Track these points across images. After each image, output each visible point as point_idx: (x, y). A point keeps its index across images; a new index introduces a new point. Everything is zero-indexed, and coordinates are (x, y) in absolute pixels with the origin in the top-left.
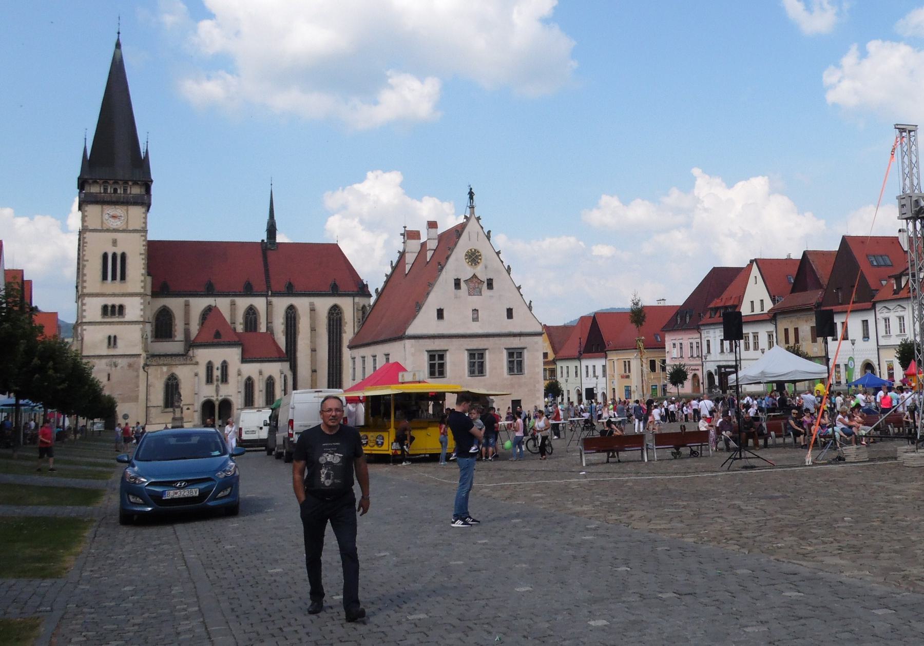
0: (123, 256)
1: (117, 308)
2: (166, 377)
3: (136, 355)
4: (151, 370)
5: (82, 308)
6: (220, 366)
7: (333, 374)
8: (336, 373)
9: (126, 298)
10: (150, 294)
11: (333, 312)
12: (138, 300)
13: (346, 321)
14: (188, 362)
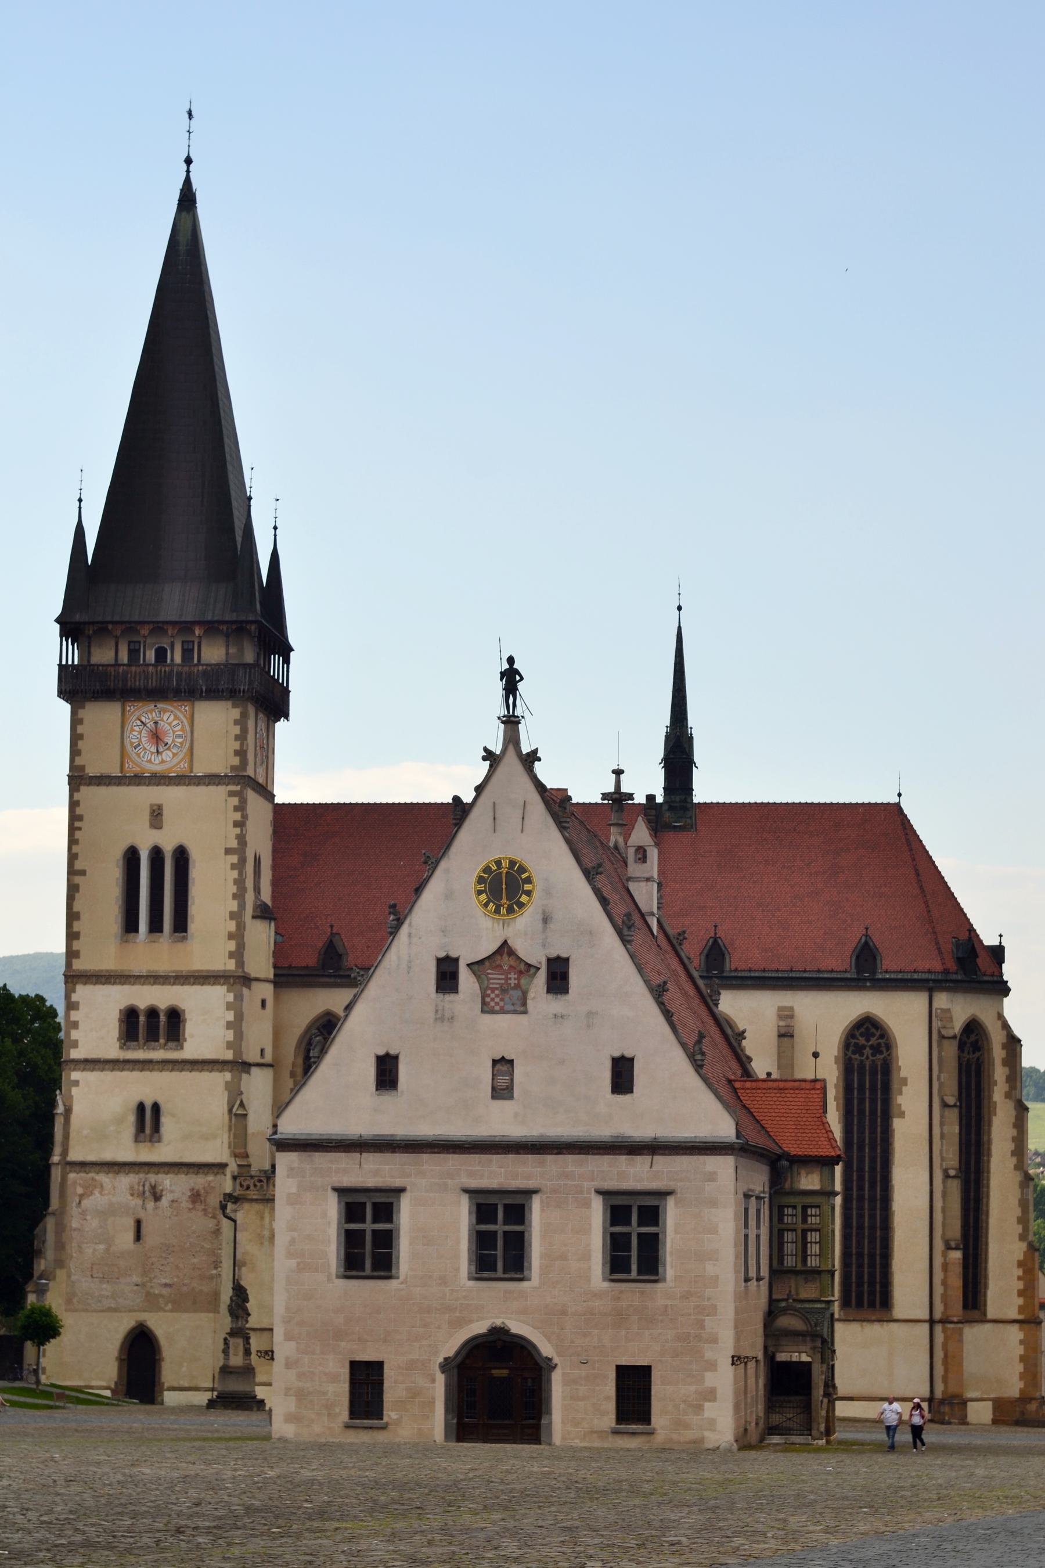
1: (163, 1018)
7: (860, 1255)
8: (872, 1256)
10: (271, 976)
11: (862, 1041)
12: (218, 995)
13: (903, 1074)
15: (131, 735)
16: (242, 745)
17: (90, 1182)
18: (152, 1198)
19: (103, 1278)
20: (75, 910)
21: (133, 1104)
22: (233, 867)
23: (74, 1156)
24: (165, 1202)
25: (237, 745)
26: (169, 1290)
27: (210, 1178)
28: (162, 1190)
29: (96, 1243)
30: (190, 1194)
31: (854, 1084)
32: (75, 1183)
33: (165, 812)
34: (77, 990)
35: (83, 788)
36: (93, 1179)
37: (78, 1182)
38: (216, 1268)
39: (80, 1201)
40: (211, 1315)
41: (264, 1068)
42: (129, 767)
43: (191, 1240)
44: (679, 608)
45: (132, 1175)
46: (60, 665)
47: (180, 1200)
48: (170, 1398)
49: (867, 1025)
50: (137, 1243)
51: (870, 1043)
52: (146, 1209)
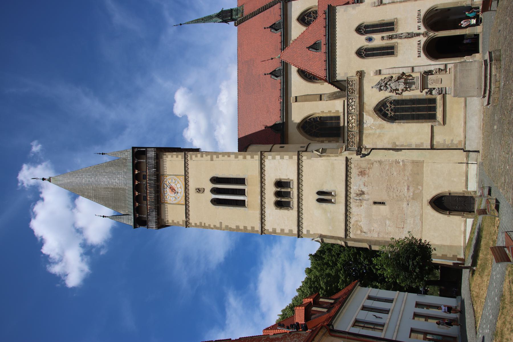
0: (215, 180)
2: (380, 121)
3: (347, 166)
4: (367, 143)
5: (279, 233)
6: (364, 37)
9: (266, 178)
15: (172, 200)
16: (174, 155)
17: (355, 227)
18: (363, 196)
19: (404, 222)
20: (235, 228)
21: (318, 204)
22: (218, 157)
23: (342, 235)
24: (365, 189)
25: (175, 156)
26: (410, 188)
27: (352, 166)
28: (359, 191)
29: (386, 225)
30: (361, 176)
32: (355, 234)
33: (198, 187)
34: (267, 229)
35: (191, 221)
36: (353, 225)
37: (354, 233)
38: (399, 163)
39: (364, 232)
40: (425, 165)
42: (183, 202)
43: (384, 176)
44: (181, 24)
45: (351, 206)
47: (364, 182)
48: (473, 187)
50: (386, 204)
52: (368, 199)
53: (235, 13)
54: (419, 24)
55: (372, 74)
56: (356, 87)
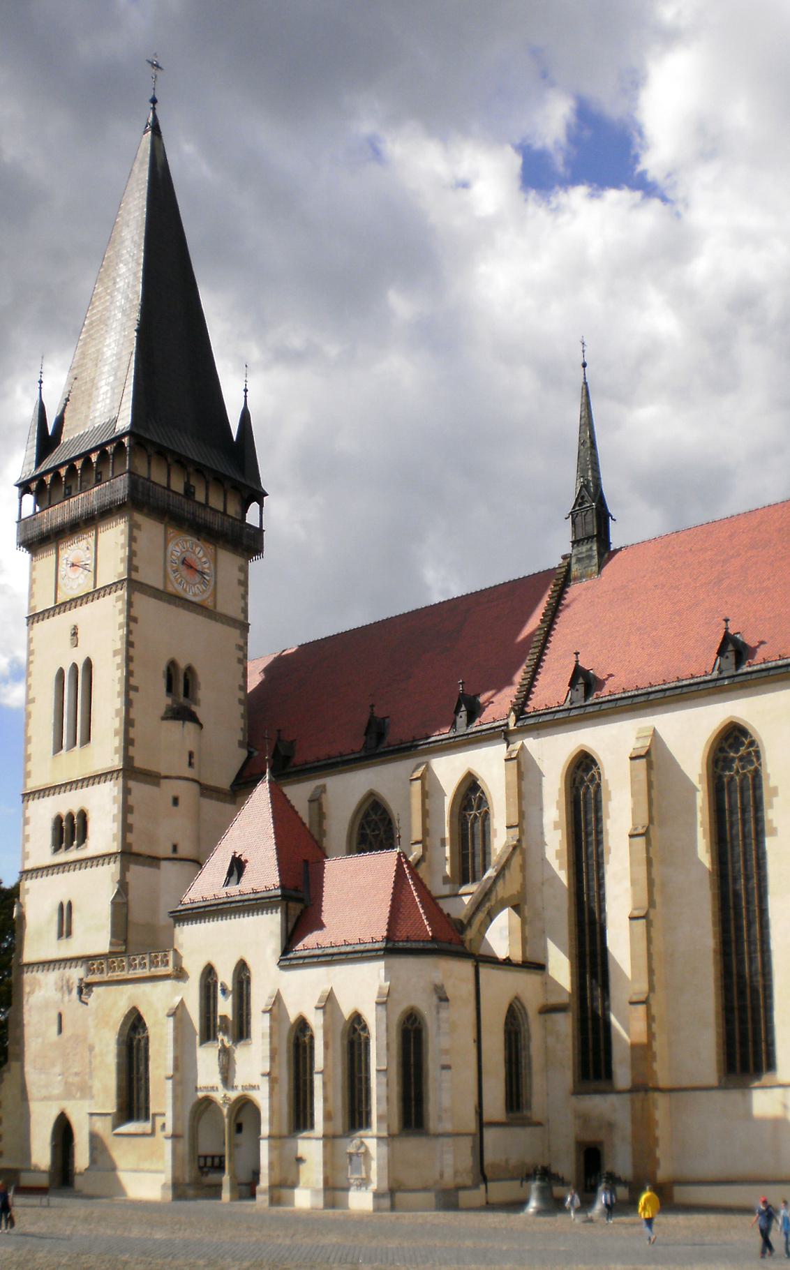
14: (161, 970)
18: (67, 992)
31: (724, 805)
35: (35, 625)
36: (35, 978)
41: (175, 862)
45: (56, 971)
46: (20, 521)
49: (734, 734)
51: (740, 754)
53: (581, 553)
54: (240, 1088)
55: (177, 1000)
56: (161, 970)
